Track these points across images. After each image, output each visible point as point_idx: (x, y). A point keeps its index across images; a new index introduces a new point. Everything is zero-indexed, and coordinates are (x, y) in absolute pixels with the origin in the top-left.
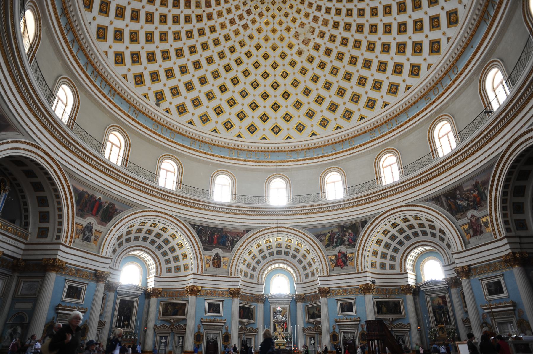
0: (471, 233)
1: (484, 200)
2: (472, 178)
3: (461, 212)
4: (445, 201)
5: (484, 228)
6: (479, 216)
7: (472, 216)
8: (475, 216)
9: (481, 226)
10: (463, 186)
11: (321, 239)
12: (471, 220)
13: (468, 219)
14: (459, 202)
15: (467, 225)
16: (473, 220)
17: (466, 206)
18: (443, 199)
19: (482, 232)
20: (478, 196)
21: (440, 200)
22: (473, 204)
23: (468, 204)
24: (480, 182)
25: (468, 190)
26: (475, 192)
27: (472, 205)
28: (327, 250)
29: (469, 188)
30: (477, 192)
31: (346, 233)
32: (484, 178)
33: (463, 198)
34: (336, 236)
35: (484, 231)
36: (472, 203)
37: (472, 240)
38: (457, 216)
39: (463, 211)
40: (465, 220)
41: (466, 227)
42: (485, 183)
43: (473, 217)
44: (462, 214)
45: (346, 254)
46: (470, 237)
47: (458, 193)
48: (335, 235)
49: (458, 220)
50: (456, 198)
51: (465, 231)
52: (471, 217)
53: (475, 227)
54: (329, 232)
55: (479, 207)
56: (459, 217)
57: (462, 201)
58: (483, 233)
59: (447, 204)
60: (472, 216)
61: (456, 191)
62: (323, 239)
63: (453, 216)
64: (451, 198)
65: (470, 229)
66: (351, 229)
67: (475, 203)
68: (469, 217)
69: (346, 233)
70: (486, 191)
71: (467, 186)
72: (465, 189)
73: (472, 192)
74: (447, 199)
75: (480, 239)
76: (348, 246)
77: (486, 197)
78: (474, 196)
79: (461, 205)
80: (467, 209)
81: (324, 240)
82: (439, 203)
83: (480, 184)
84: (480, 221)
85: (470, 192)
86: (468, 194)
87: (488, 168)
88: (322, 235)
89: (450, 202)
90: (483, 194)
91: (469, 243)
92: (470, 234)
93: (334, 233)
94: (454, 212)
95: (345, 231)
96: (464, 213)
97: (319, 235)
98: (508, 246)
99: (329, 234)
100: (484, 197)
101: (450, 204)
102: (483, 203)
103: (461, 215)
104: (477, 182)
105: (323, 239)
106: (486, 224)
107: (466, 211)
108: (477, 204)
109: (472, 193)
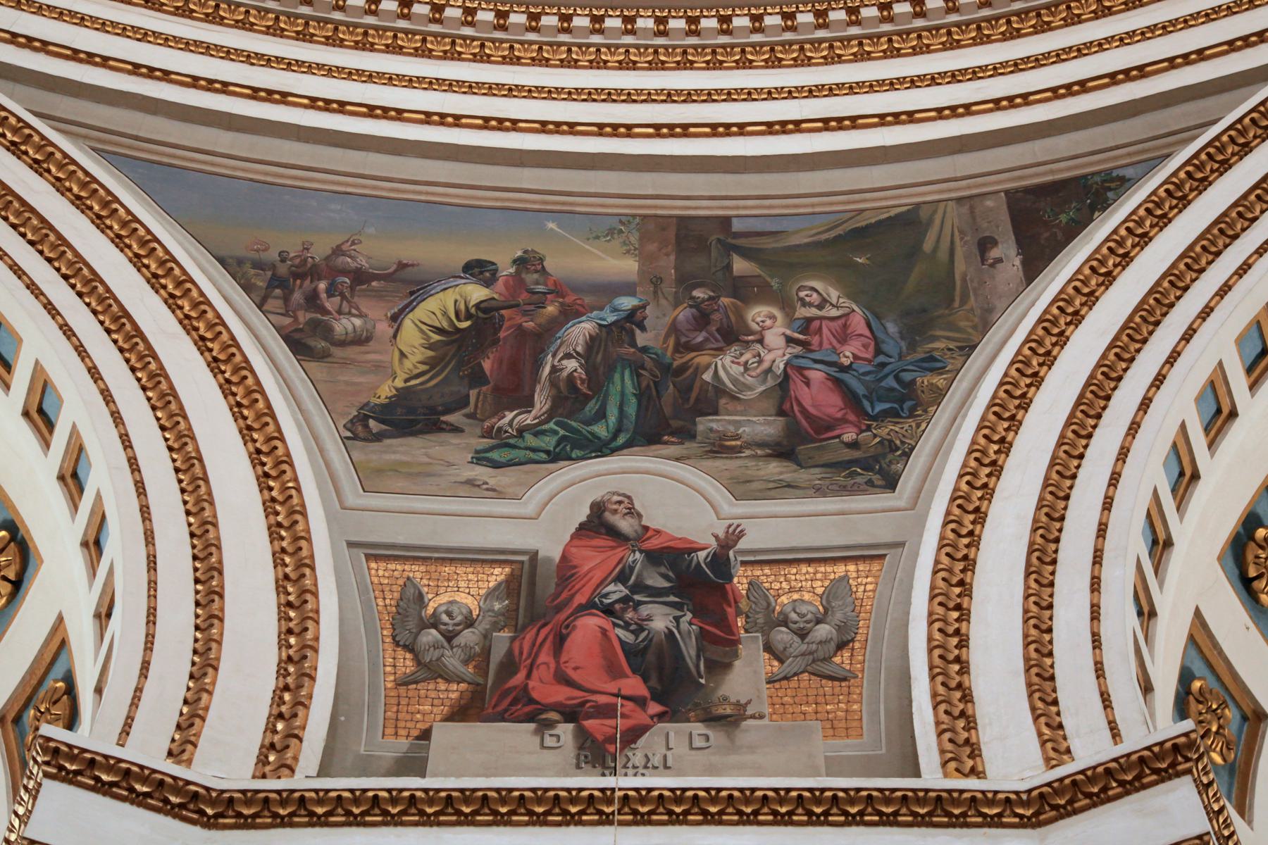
11: (323, 330)
28: (370, 479)
31: (758, 314)
34: (580, 331)
45: (720, 562)
48: (570, 313)
54: (478, 270)
62: (345, 325)
66: (839, 270)
69: (758, 314)
76: (774, 469)
81: (361, 340)
88: (360, 277)
93: (558, 290)
95: (744, 291)
97: (305, 271)
99: (476, 293)
105: (345, 325)
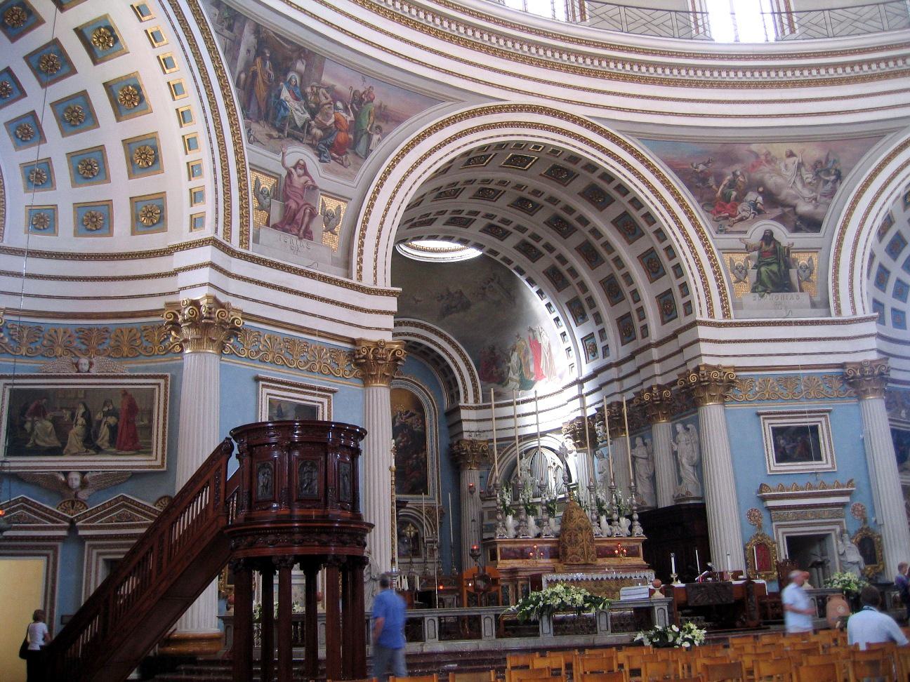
0: (276, 214)
1: (357, 154)
2: (365, 74)
3: (273, 126)
4: (249, 51)
5: (318, 226)
6: (319, 183)
7: (300, 165)
8: (306, 173)
9: (313, 215)
10: (328, 65)
12: (289, 174)
13: (283, 164)
14: (285, 94)
15: (273, 181)
16: (298, 181)
17: (299, 123)
18: (248, 39)
19: (308, 235)
20: (347, 131)
21: (235, 30)
22: (321, 139)
23: (307, 127)
24: (376, 102)
25: (330, 89)
26: (346, 110)
27: (314, 137)
29: (339, 86)
30: (351, 117)
32: (393, 103)
33: (304, 95)
35: (315, 235)
36: (319, 132)
37: (271, 237)
38: (255, 126)
39: (281, 130)
40: (270, 160)
41: (267, 184)
42: (388, 118)
43: (301, 172)
44: (275, 134)
46: (268, 224)
47: (300, 66)
49: (250, 142)
50: (286, 74)
51: (258, 193)
52: (295, 168)
53: (294, 206)
55: (334, 159)
56: (259, 137)
57: (297, 99)
58: (311, 239)
59: (248, 65)
60: (300, 165)
61: (300, 58)
63: (246, 116)
64: (270, 59)
65: (276, 197)
67: (329, 141)
68: (291, 161)
70: (376, 137)
71: (335, 77)
72: (326, 79)
73: (339, 104)
74: (259, 53)
75: (296, 251)
77: (368, 152)
78: (336, 122)
79: (286, 109)
80: (297, 134)
82: (227, 33)
83: (371, 107)
84: (316, 201)
85: (335, 100)
86: (324, 101)
87: (427, 96)
89: (258, 67)
90: (365, 137)
91: (256, 240)
92: (269, 212)
94: (254, 108)
96: (279, 137)
98: (389, 321)
100: (361, 147)
101: (255, 74)
102: (350, 157)
103: (271, 137)
104: (368, 92)
106: (330, 219)
107: (289, 135)
108: (330, 147)
109: (336, 108)
